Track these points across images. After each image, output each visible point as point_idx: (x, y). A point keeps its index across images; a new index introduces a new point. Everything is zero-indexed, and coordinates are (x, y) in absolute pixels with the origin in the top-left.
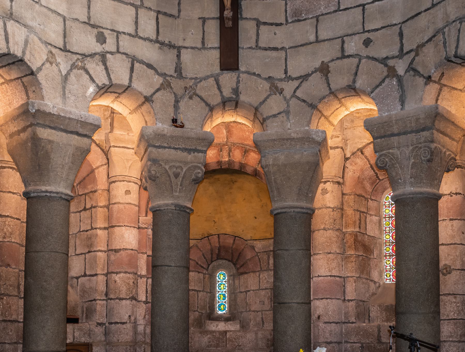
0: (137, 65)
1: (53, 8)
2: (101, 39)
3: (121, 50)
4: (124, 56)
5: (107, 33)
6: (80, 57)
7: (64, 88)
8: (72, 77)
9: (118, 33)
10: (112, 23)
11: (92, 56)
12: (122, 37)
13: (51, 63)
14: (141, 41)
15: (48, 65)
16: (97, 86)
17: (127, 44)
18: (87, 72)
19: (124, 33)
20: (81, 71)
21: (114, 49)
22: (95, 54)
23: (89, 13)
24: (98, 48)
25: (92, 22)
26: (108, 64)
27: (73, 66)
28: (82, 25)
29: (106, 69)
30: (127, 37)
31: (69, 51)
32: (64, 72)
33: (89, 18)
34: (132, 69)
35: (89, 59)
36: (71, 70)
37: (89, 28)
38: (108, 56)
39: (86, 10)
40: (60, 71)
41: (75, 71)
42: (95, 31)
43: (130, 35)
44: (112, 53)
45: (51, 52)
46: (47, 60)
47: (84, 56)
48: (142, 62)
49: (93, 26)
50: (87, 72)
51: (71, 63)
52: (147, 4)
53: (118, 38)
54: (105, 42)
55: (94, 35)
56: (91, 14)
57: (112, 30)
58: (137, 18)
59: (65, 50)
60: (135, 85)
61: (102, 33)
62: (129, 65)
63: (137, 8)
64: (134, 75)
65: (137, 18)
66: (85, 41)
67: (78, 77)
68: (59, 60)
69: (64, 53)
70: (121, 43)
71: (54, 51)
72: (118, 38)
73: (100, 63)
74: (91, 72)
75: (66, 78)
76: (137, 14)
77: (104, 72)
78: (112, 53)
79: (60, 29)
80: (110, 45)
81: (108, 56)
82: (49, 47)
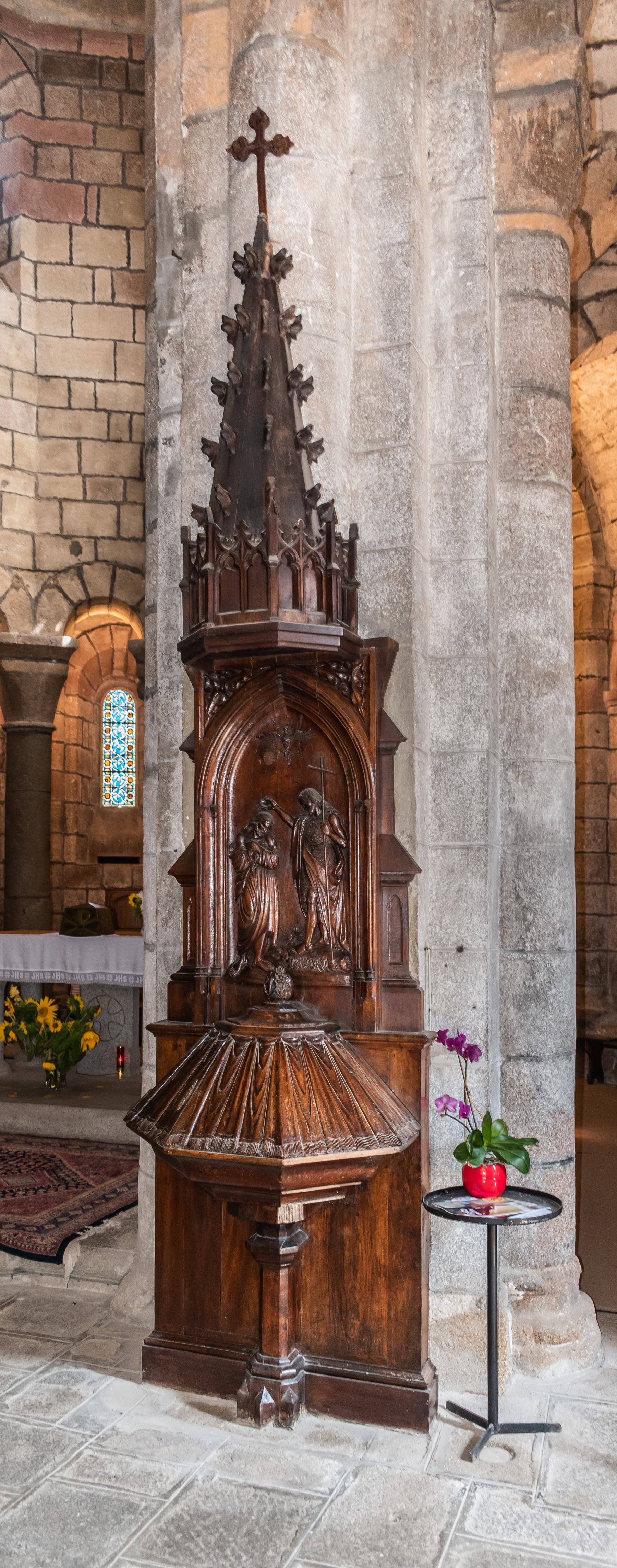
0: (119, 572)
1: (18, 527)
2: (76, 549)
3: (100, 557)
4: (104, 565)
5: (82, 542)
6: (52, 574)
7: (34, 613)
8: (44, 598)
9: (96, 538)
10: (88, 529)
11: (66, 570)
12: (100, 543)
13: (17, 589)
14: (124, 543)
15: (13, 592)
16: (71, 602)
17: (106, 550)
18: (61, 590)
19: (103, 538)
20: (55, 591)
21: (91, 558)
22: (70, 568)
23: (61, 523)
24: (72, 560)
25: (65, 533)
26: (85, 577)
27: (45, 586)
28: (54, 539)
29: (83, 582)
30: (107, 541)
31: (39, 570)
32: (33, 595)
33: (61, 529)
34: (113, 578)
35: (62, 575)
36: (42, 590)
37: (62, 540)
38: (86, 567)
39: (58, 520)
40: (29, 595)
41: (47, 591)
42: (69, 542)
43: (110, 538)
44: (89, 563)
45: (17, 577)
46: (12, 586)
47: (57, 572)
48: (125, 567)
49: (66, 537)
50: (61, 590)
51: (42, 582)
52: (131, 498)
53: (96, 545)
54: (80, 552)
55: (67, 547)
56: (64, 523)
57: (89, 537)
58: (119, 517)
59: (35, 570)
60: (117, 595)
61: (78, 543)
62: (110, 573)
63: (118, 505)
64: (116, 583)
65: (119, 517)
66: (58, 555)
67: (50, 597)
68: (26, 582)
69: (33, 574)
70: (100, 550)
71: (20, 574)
72: (96, 545)
73: (76, 578)
74: (65, 589)
75: (36, 601)
76: (119, 512)
77: (80, 586)
78: (89, 563)
79: (27, 548)
80: (87, 554)
81: (86, 567)
82: (14, 571)
